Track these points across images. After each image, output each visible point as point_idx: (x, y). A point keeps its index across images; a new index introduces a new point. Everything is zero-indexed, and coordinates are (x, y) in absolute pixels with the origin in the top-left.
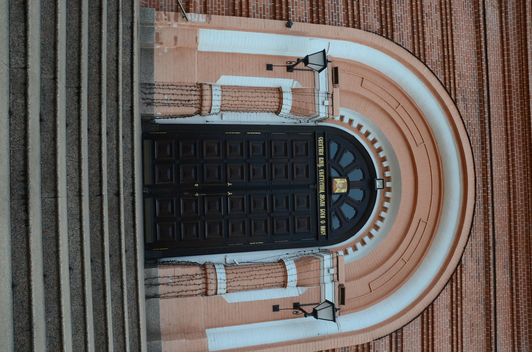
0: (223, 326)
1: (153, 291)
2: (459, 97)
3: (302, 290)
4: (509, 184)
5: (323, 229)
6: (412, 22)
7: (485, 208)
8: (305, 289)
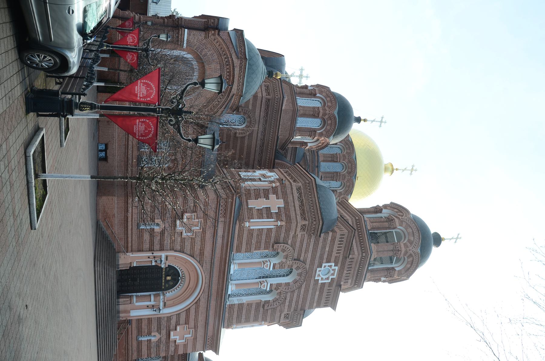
0: (134, 310)
1: (118, 304)
2: (204, 262)
4: (218, 282)
5: (163, 287)
6: (191, 246)
7: (209, 287)
8: (156, 302)
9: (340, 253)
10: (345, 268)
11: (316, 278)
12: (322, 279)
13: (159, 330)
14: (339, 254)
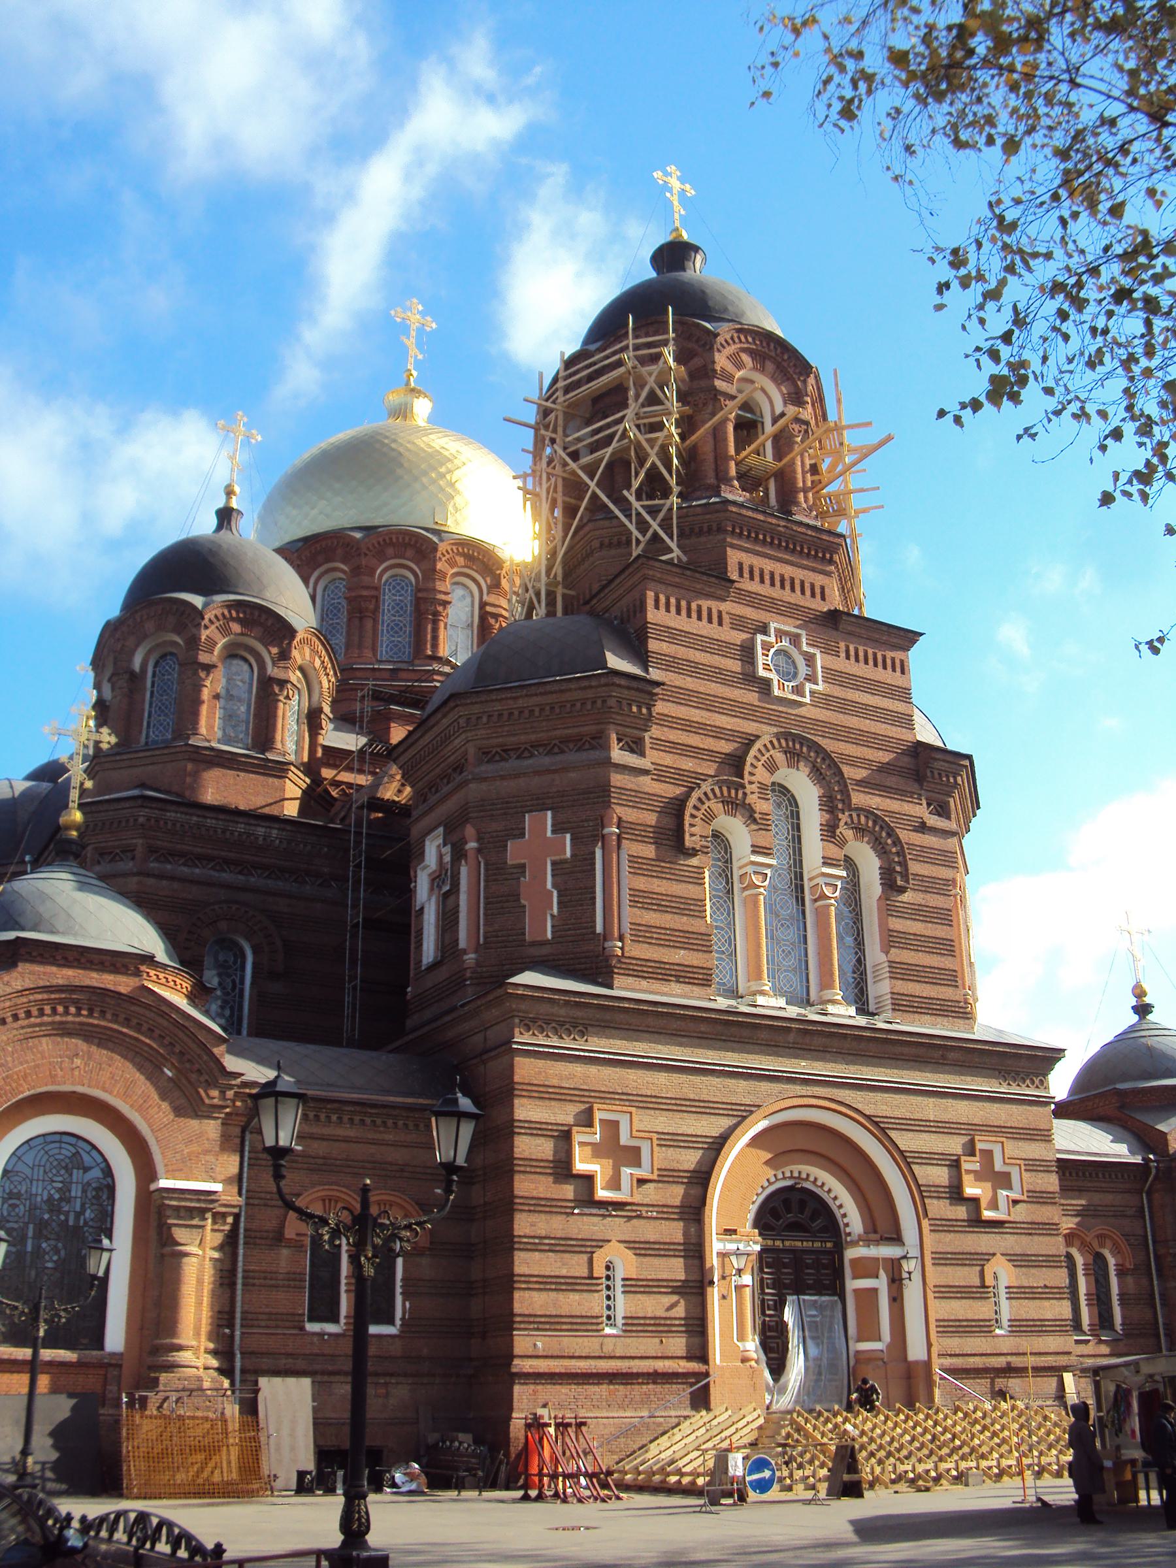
3: (882, 1273)
5: (829, 1245)
9: (720, 613)
10: (775, 595)
11: (807, 700)
13: (980, 1260)
14: (725, 616)
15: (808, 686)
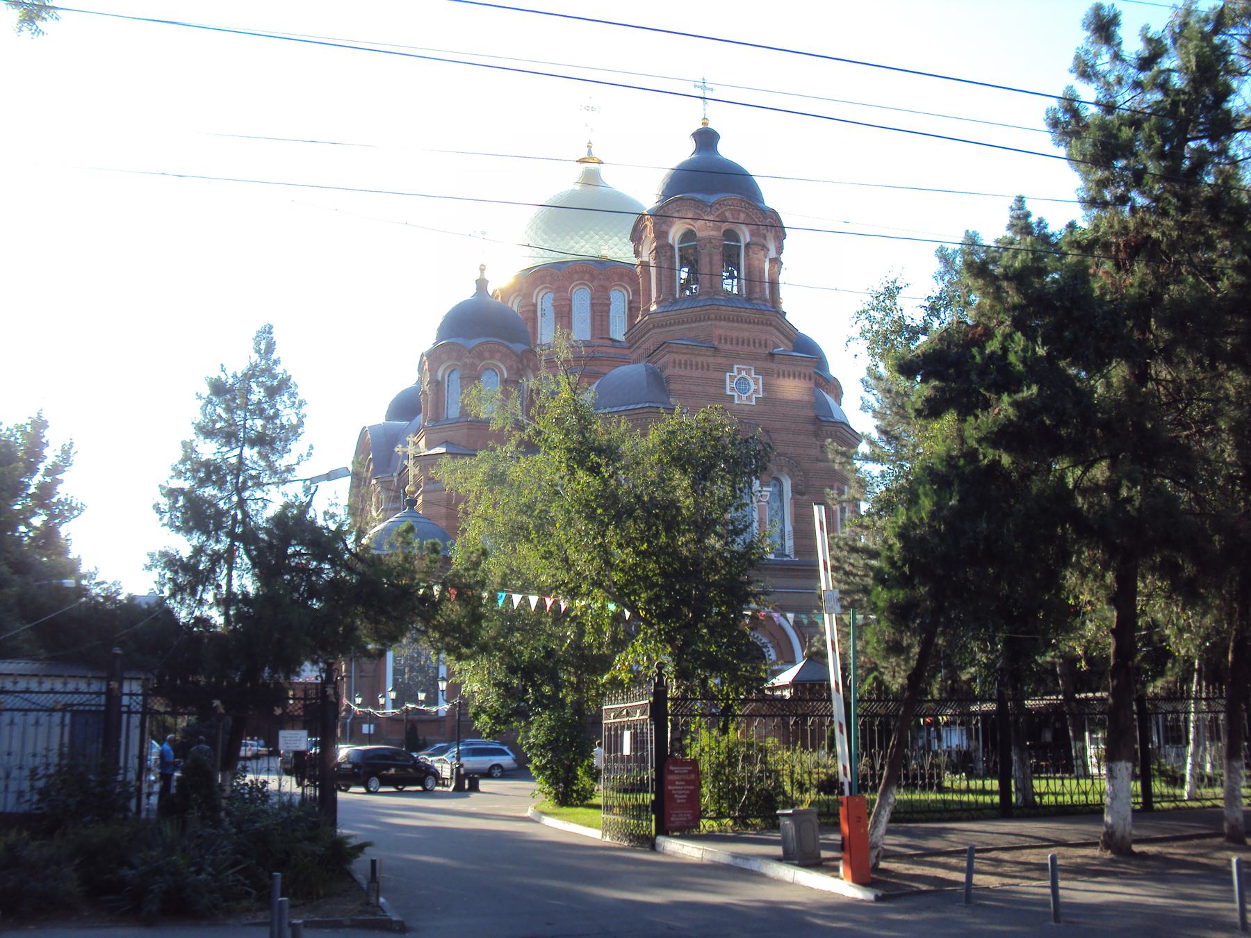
11: (754, 403)
12: (756, 391)
15: (754, 396)
